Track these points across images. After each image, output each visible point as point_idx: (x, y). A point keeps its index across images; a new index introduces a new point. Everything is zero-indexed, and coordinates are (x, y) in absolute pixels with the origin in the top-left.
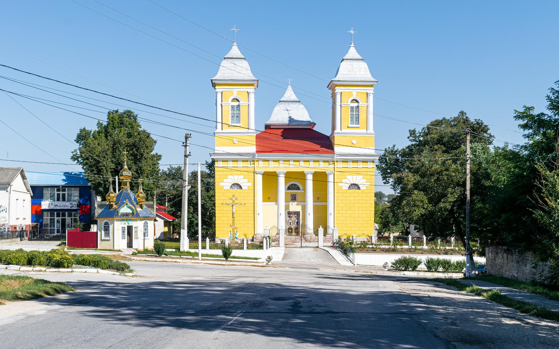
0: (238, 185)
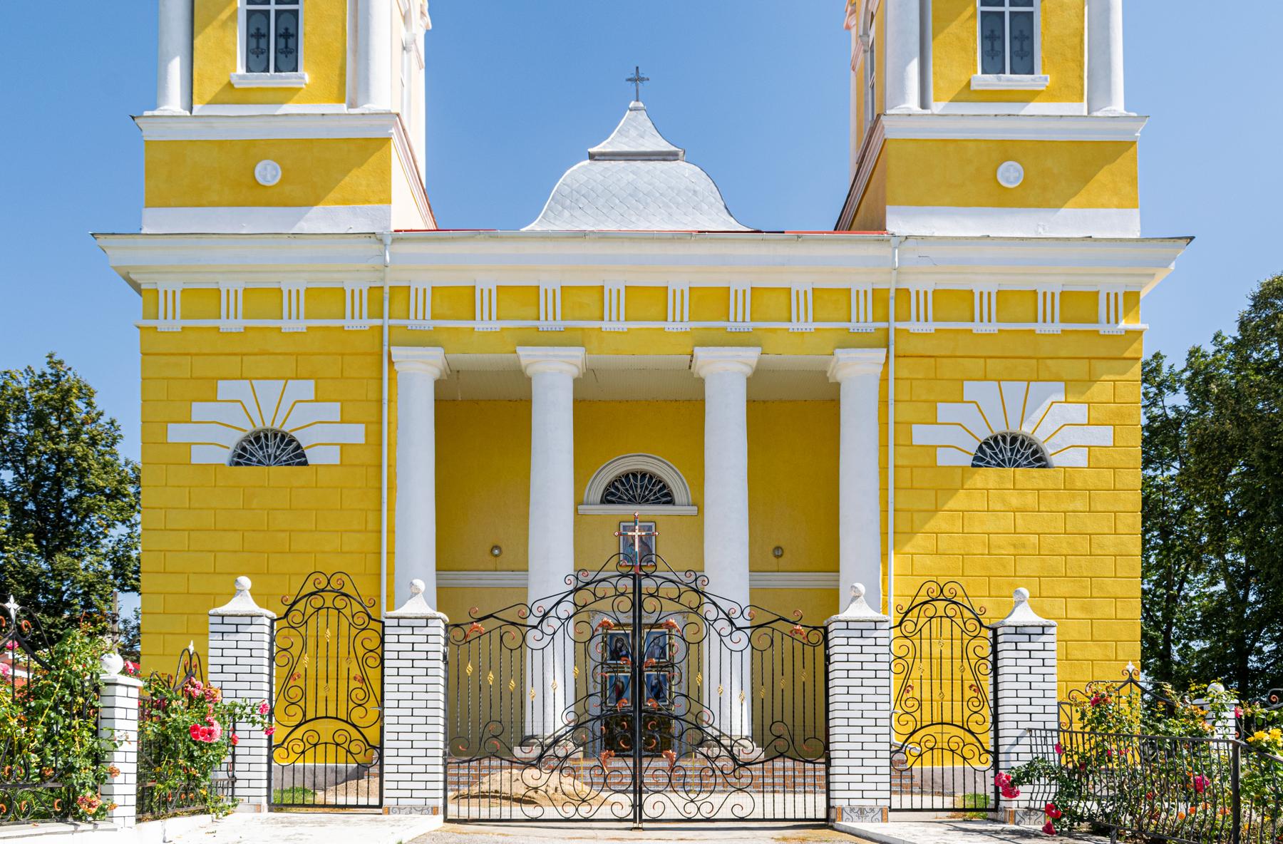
0: (285, 440)
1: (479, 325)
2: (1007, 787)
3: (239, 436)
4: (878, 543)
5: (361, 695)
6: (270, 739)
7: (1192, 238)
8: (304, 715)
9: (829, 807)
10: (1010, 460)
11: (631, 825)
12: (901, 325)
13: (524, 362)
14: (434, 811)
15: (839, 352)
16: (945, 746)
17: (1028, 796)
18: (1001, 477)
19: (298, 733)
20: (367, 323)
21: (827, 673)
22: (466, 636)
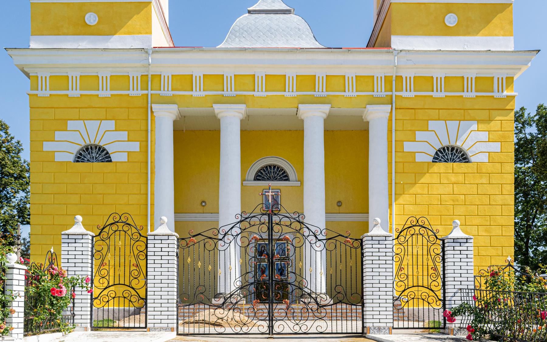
0: (101, 150)
1: (194, 94)
2: (450, 317)
3: (78, 148)
4: (388, 199)
5: (136, 273)
6: (92, 295)
7: (539, 51)
8: (109, 283)
9: (363, 327)
10: (451, 159)
11: (268, 336)
12: (398, 94)
13: (216, 111)
14: (172, 330)
15: (368, 106)
16: (420, 297)
17: (460, 322)
18: (447, 167)
19: (105, 292)
20: (141, 92)
21: (362, 261)
22: (187, 244)
